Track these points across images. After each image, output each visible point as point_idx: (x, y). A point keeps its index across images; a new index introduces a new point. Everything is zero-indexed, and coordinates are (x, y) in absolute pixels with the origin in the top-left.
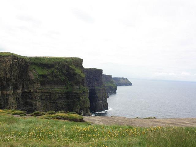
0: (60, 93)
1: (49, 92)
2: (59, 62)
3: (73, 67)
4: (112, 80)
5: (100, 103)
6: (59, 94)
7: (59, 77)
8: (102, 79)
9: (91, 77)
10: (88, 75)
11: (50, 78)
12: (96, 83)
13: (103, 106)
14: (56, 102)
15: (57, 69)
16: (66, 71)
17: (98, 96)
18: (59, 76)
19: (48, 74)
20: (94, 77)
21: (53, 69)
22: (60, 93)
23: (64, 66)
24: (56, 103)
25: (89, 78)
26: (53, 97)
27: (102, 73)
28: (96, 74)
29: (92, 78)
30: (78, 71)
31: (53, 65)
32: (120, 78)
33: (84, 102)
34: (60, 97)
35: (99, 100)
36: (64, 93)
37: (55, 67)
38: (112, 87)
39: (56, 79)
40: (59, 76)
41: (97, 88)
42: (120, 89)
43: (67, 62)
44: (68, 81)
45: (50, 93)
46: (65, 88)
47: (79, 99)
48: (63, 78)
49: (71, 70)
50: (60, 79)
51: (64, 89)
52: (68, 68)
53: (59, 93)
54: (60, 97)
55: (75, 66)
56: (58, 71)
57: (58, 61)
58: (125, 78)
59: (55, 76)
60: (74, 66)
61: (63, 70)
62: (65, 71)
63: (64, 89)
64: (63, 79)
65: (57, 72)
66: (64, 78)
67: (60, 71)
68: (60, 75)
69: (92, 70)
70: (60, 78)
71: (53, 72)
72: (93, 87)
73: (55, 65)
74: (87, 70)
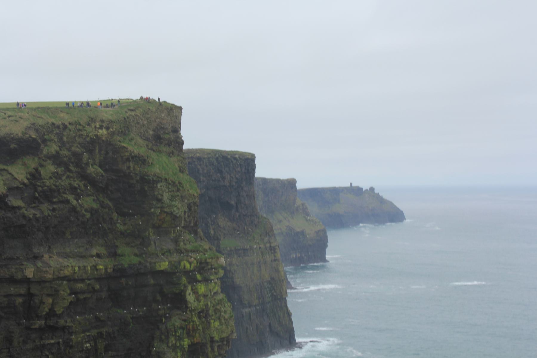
0: (82, 280)
1: (19, 276)
2: (65, 127)
3: (136, 146)
4: (299, 202)
6: (80, 286)
7: (67, 202)
8: (252, 196)
11: (19, 208)
12: (223, 221)
14: (62, 322)
15: (56, 158)
16: (100, 166)
18: (71, 198)
19: (10, 189)
21: (32, 163)
22: (82, 280)
23: (92, 145)
24: (64, 328)
26: (42, 302)
27: (254, 170)
28: (224, 178)
30: (161, 165)
31: (34, 139)
32: (335, 191)
33: (204, 314)
34: (81, 297)
36: (99, 279)
37: (45, 152)
38: (303, 233)
39: (54, 210)
40: (71, 198)
42: (340, 246)
43: (107, 125)
44: (115, 216)
45: (27, 281)
46: (103, 251)
47: (179, 301)
48: (88, 202)
49: (128, 160)
50: (74, 209)
51: (98, 256)
53: (76, 281)
55: (147, 139)
56: (60, 170)
58: (365, 186)
59: (48, 195)
60: (140, 141)
61: (87, 164)
62: (93, 170)
63: (98, 256)
64: (92, 211)
65: (56, 176)
66: (95, 206)
67: (72, 168)
68: (73, 190)
69: (199, 159)
70: (75, 202)
71: (35, 176)
73: (44, 141)
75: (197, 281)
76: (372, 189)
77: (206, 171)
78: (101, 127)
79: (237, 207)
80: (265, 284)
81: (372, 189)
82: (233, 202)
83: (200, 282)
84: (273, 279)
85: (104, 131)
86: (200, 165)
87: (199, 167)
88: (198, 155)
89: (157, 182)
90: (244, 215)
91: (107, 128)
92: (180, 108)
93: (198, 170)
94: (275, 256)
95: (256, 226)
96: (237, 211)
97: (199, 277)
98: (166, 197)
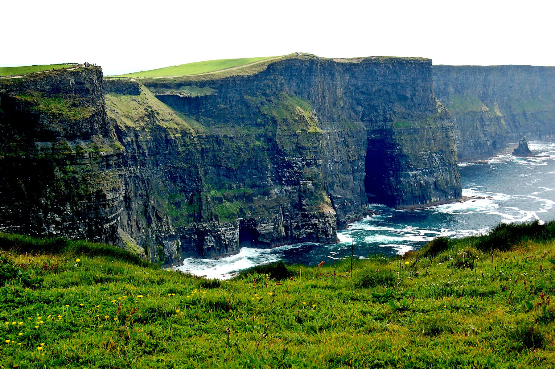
5: (415, 176)
9: (375, 89)
10: (360, 83)
12: (398, 107)
13: (435, 184)
17: (405, 151)
20: (389, 89)
25: (362, 93)
28: (399, 78)
29: (379, 90)
35: (411, 166)
41: (398, 125)
52: (8, 102)
72: (385, 120)
74: (352, 64)
75: (67, 165)
77: (382, 73)
79: (412, 99)
80: (434, 155)
82: (408, 95)
84: (442, 151)
86: (377, 69)
87: (376, 70)
88: (375, 61)
89: (40, 114)
90: (419, 104)
91: (5, 89)
93: (375, 73)
94: (446, 134)
95: (432, 112)
96: (412, 101)
97: (68, 162)
98: (45, 122)
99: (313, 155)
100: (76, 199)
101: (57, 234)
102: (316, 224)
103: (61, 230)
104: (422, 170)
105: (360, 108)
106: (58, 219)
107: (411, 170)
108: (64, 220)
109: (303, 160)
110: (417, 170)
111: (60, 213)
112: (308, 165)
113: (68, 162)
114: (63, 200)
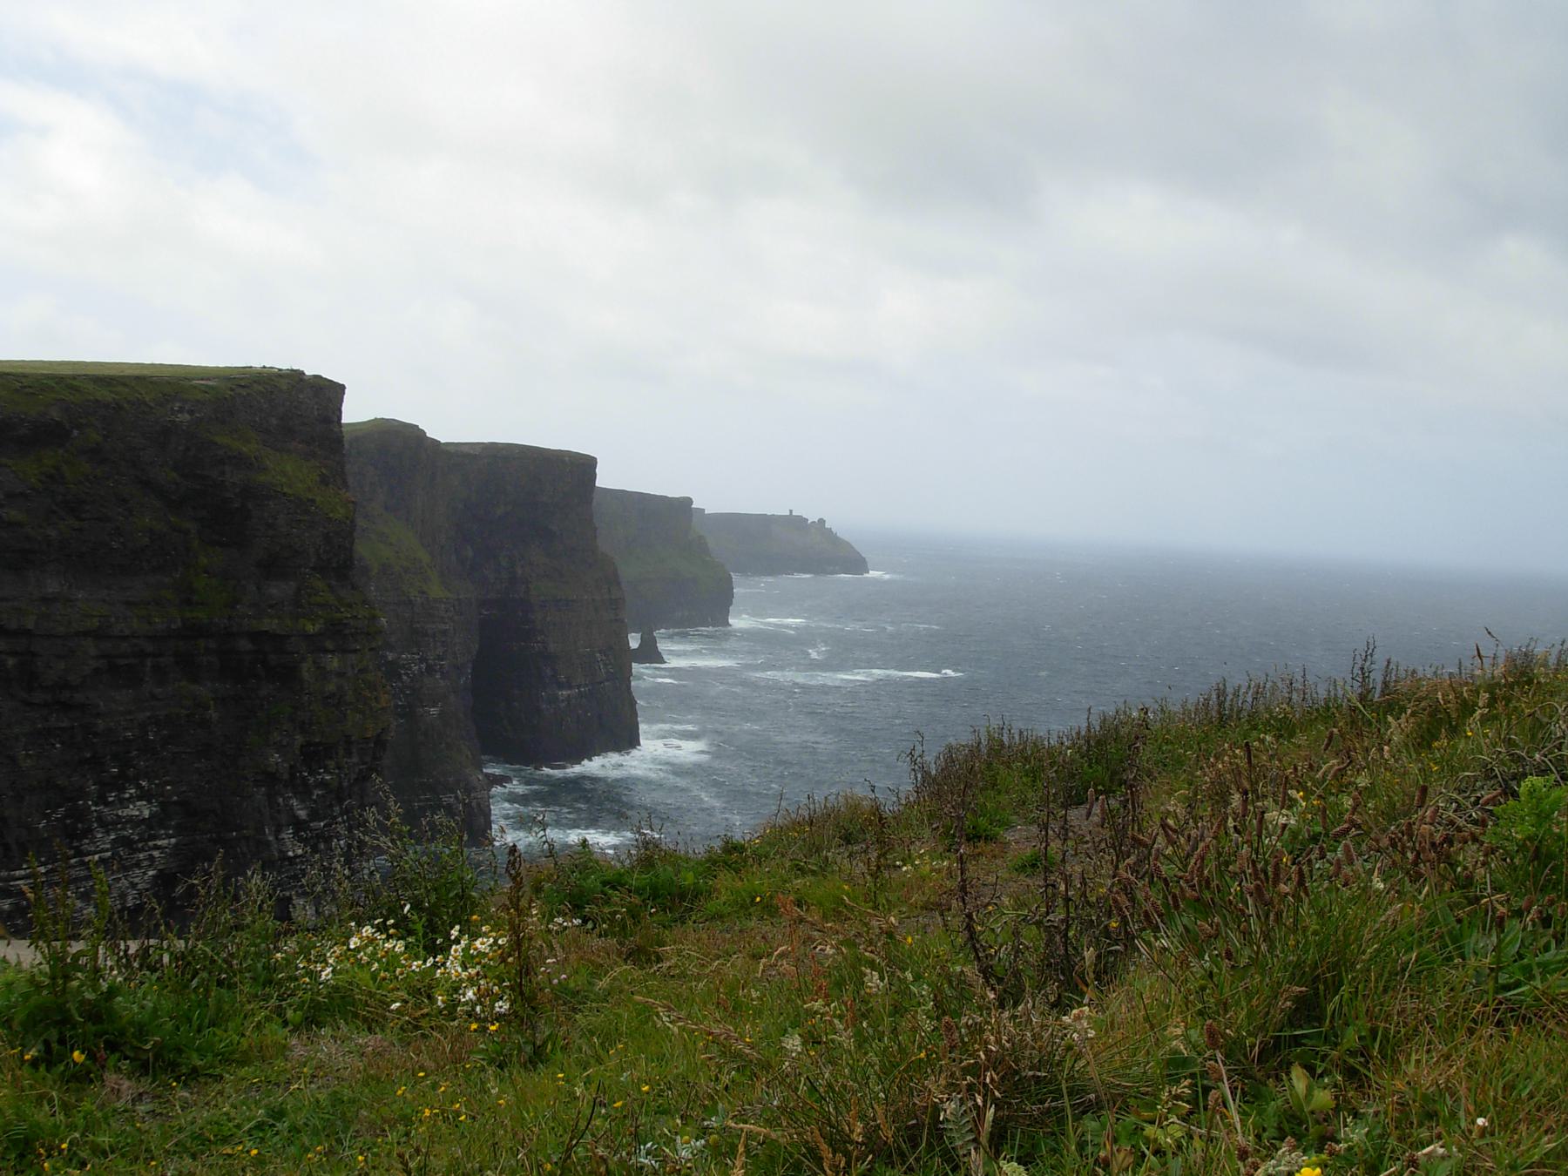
32: (765, 521)
34: (122, 662)
35: (562, 678)
45: (28, 633)
54: (122, 662)
57: (104, 394)
58: (812, 517)
75: (326, 651)
76: (822, 521)
78: (181, 410)
81: (822, 521)
83: (332, 652)
85: (187, 417)
91: (191, 412)
92: (342, 387)
97: (329, 645)
99: (440, 651)
100: (341, 752)
101: (296, 856)
102: (450, 806)
103: (304, 841)
104: (579, 687)
105: (470, 553)
106: (302, 814)
107: (561, 686)
108: (314, 815)
109: (422, 660)
110: (570, 687)
111: (304, 792)
112: (430, 670)
113: (329, 645)
114: (314, 755)
